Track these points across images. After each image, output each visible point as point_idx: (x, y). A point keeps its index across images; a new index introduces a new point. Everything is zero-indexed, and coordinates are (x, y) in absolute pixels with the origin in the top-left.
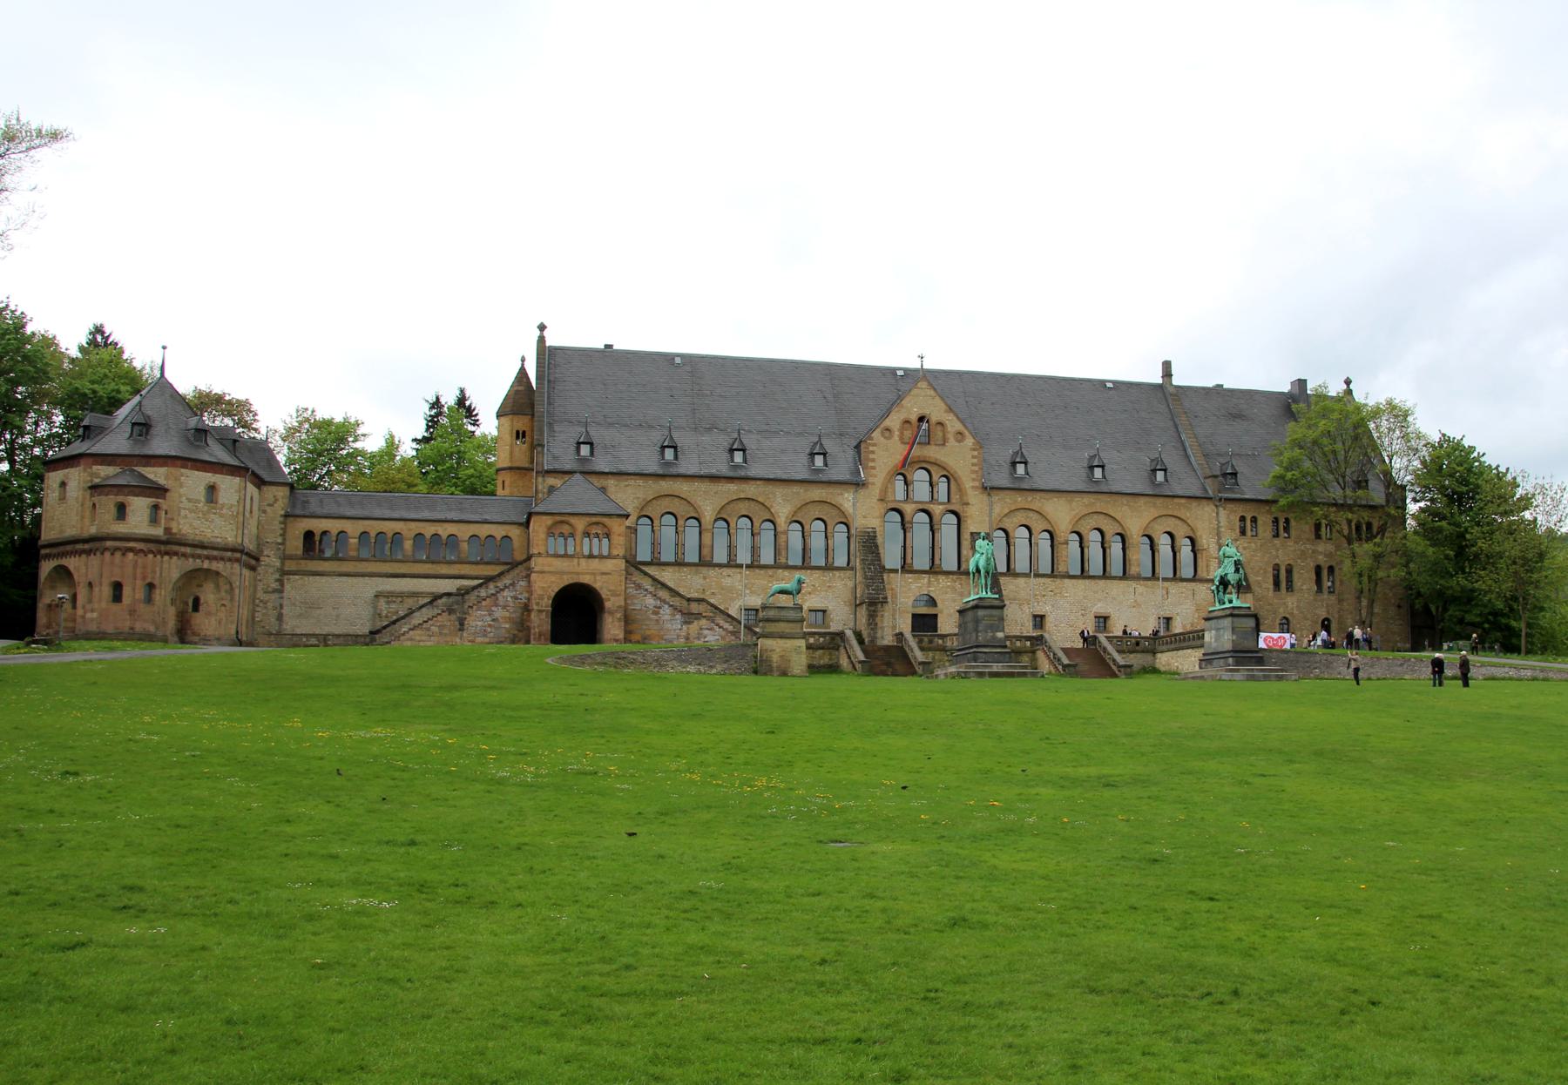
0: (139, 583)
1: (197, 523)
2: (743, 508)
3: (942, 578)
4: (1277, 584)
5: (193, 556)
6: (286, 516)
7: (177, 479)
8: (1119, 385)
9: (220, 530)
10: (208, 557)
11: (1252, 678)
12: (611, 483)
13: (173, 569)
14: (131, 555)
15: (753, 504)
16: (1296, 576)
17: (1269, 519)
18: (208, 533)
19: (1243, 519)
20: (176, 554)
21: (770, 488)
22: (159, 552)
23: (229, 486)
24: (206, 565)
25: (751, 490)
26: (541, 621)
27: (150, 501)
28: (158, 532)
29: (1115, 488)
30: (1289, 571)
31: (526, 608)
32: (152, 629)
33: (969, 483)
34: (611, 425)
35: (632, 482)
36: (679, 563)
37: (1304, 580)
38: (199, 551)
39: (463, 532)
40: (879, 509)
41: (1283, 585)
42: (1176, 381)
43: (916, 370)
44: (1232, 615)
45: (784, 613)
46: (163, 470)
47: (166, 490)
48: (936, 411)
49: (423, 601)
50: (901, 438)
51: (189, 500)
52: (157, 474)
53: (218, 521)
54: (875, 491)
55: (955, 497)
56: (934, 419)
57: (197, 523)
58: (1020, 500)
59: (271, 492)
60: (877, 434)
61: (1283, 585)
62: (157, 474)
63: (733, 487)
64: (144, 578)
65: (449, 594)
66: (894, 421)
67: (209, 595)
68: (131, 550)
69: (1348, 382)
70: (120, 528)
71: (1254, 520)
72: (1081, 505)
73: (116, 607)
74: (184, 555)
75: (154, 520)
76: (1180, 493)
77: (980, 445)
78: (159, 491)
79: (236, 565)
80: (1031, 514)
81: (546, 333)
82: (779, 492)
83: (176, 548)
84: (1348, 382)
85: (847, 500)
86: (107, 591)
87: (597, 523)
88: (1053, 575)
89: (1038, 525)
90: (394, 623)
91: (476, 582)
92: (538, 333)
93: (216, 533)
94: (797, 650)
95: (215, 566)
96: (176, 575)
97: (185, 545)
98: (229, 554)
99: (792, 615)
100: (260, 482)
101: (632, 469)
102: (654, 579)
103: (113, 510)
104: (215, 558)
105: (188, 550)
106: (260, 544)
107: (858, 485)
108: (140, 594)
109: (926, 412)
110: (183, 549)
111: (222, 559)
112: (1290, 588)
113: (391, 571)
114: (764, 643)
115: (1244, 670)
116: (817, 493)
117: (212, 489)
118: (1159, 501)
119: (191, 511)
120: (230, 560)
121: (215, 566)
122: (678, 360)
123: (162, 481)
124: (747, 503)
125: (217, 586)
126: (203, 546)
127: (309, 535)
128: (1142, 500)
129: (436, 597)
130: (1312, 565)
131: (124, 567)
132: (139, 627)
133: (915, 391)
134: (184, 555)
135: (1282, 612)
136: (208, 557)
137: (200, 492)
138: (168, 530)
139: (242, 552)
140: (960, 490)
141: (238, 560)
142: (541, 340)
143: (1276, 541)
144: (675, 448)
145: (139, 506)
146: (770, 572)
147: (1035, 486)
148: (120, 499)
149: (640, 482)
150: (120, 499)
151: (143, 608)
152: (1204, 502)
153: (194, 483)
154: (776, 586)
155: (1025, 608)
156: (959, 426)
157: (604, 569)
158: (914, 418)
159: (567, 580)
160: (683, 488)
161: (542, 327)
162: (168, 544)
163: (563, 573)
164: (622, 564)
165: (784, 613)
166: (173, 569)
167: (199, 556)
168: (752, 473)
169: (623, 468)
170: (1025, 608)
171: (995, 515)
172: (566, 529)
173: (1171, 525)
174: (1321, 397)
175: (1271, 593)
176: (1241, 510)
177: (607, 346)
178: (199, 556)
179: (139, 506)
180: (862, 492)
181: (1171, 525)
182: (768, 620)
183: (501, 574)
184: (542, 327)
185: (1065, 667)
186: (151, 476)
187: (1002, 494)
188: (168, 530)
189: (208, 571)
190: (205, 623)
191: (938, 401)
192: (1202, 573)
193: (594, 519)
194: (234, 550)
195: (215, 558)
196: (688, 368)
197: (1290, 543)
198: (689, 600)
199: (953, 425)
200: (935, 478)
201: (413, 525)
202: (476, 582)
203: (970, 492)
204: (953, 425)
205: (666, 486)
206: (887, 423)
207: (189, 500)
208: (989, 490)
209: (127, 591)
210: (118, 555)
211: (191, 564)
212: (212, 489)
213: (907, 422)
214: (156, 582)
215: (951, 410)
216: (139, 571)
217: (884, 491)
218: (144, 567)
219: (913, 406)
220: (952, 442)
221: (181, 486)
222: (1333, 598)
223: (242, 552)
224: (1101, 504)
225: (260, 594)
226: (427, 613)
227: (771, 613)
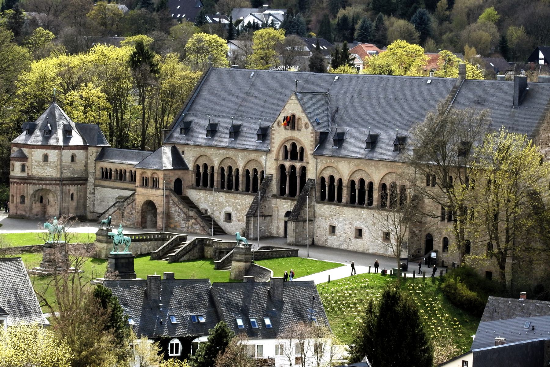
0: (18, 195)
10: (44, 184)
18: (45, 174)
20: (30, 183)
24: (44, 187)
28: (25, 175)
38: (40, 182)
51: (36, 161)
53: (49, 169)
64: (20, 193)
74: (34, 184)
79: (58, 186)
83: (31, 181)
93: (48, 174)
95: (48, 187)
96: (31, 192)
97: (34, 180)
98: (54, 182)
105: (36, 182)
108: (19, 200)
110: (34, 181)
111: (51, 184)
117: (46, 157)
119: (37, 166)
120: (54, 184)
121: (48, 187)
126: (41, 179)
134: (34, 184)
136: (44, 184)
139: (60, 181)
141: (58, 184)
166: (30, 189)
167: (41, 184)
178: (41, 184)
194: (56, 180)
195: (46, 184)
207: (36, 161)
214: (25, 195)
218: (20, 189)
220: (303, 129)
221: (32, 156)
225: (88, 195)
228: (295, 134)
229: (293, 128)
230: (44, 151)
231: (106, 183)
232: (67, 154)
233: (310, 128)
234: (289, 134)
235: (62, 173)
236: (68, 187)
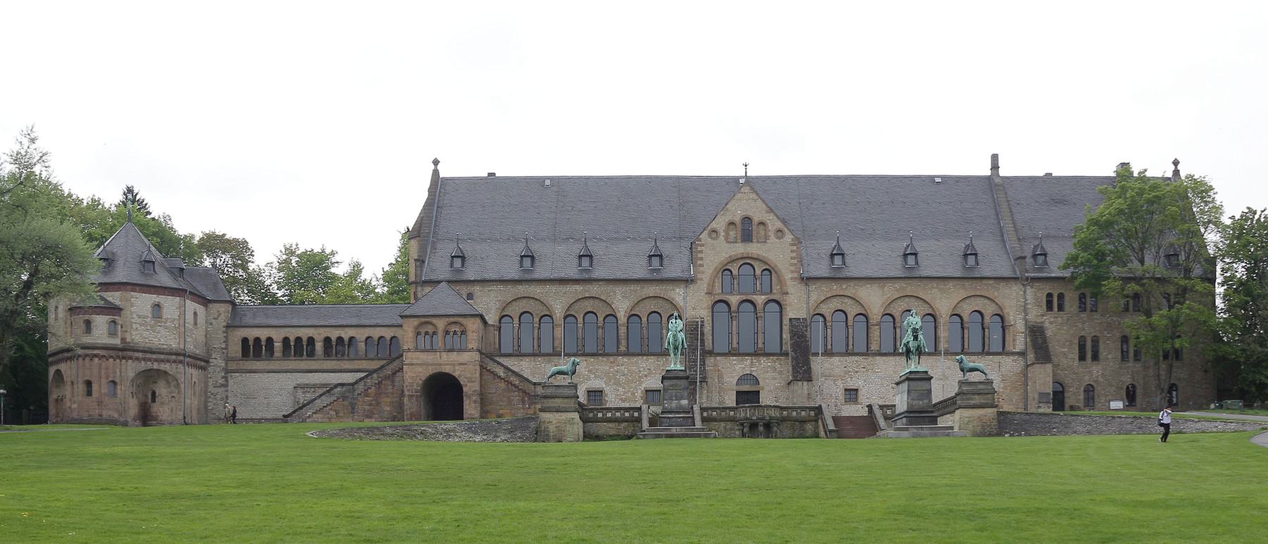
0: (104, 381)
1: (146, 334)
2: (589, 305)
3: (763, 359)
4: (1082, 357)
5: (144, 359)
6: (227, 327)
7: (128, 300)
8: (946, 179)
9: (165, 338)
10: (156, 360)
11: (915, 436)
12: (477, 289)
13: (130, 369)
14: (96, 360)
15: (597, 302)
16: (1102, 347)
17: (1076, 295)
18: (156, 341)
19: (1050, 295)
20: (131, 358)
21: (610, 287)
22: (118, 357)
23: (170, 305)
24: (156, 366)
25: (594, 290)
26: (410, 405)
27: (107, 318)
28: (116, 341)
29: (925, 273)
30: (1096, 341)
31: (402, 394)
32: (116, 416)
33: (788, 276)
34: (484, 240)
35: (494, 288)
36: (519, 354)
37: (1109, 351)
38: (149, 356)
39: (360, 335)
40: (708, 302)
41: (1089, 355)
42: (1003, 172)
43: (736, 179)
44: (908, 379)
45: (560, 391)
46: (118, 294)
47: (121, 309)
48: (758, 212)
49: (321, 391)
50: (726, 239)
51: (139, 317)
52: (114, 297)
53: (163, 332)
54: (703, 286)
55: (776, 288)
56: (756, 220)
57: (146, 334)
58: (835, 288)
59: (215, 308)
60: (704, 236)
61: (1089, 355)
62: (114, 297)
63: (579, 288)
64: (107, 377)
65: (342, 385)
66: (720, 224)
67: (162, 390)
68: (96, 356)
69: (1176, 163)
70: (87, 340)
71: (1061, 296)
72: (891, 291)
73: (89, 400)
75: (112, 334)
76: (988, 274)
77: (797, 241)
78: (114, 310)
80: (846, 300)
81: (439, 167)
82: (619, 290)
83: (130, 353)
84: (1176, 163)
85: (677, 294)
86: (81, 388)
87: (455, 323)
88: (867, 353)
89: (852, 310)
90: (301, 408)
91: (363, 375)
92: (433, 167)
94: (571, 421)
96: (131, 374)
97: (138, 351)
99: (567, 392)
100: (205, 302)
101: (493, 276)
102: (506, 368)
103: (83, 326)
104: (162, 361)
105: (140, 355)
106: (209, 350)
107: (688, 281)
109: (750, 214)
110: (136, 354)
111: (168, 361)
112: (1095, 357)
113: (356, 367)
114: (546, 416)
115: (914, 429)
116: (652, 290)
117: (157, 306)
118: (967, 283)
119: (141, 325)
122: (548, 182)
123: (118, 303)
124: (592, 301)
125: (168, 382)
126: (152, 352)
127: (245, 341)
128: (951, 284)
129: (330, 389)
130: (1118, 335)
131: (93, 369)
132: (105, 414)
133: (739, 196)
134: (137, 359)
135: (1087, 380)
136: (156, 360)
138: (123, 340)
140: (781, 282)
142: (436, 172)
143: (1083, 315)
144: (591, 257)
145: (101, 322)
146: (611, 359)
147: (849, 275)
148: (87, 317)
149: (501, 287)
150: (87, 317)
152: (1012, 283)
153: (141, 303)
154: (554, 369)
155: (840, 383)
156: (779, 225)
157: (462, 361)
158: (737, 219)
159: (431, 370)
160: (536, 290)
161: (436, 162)
162: (125, 351)
163: (428, 365)
164: (476, 356)
165: (560, 391)
166: (130, 369)
167: (150, 360)
168: (595, 275)
169: (487, 276)
170: (840, 383)
171: (812, 302)
172: (430, 329)
173: (979, 304)
174: (1142, 178)
175: (1076, 362)
176: (1047, 288)
177: (490, 174)
178: (150, 360)
179: (101, 322)
180: (692, 287)
181: (979, 304)
182: (545, 397)
183: (383, 367)
184: (436, 162)
185: (831, 431)
186: (110, 299)
187: (818, 283)
188: (123, 340)
189: (158, 370)
190: (161, 410)
191: (759, 202)
192: (1009, 348)
193: (452, 320)
195: (162, 361)
196: (555, 189)
197: (1096, 316)
198: (535, 384)
199: (774, 223)
200: (758, 272)
201: (322, 330)
202: (363, 375)
203: (789, 283)
204: (774, 223)
205: (522, 290)
206: (714, 225)
207: (139, 317)
208: (807, 280)
209: (95, 387)
210: (87, 360)
211: (143, 366)
212: (157, 306)
213: (732, 223)
214: (117, 380)
215: (771, 210)
216: (103, 372)
217: (712, 284)
218: (107, 368)
219: (736, 211)
220: (773, 238)
221: (132, 305)
222: (1138, 365)
223: (184, 355)
224: (911, 288)
226: (326, 400)
227: (549, 391)
228: (753, 249)
229: (747, 237)
233: (789, 237)
234: (741, 249)
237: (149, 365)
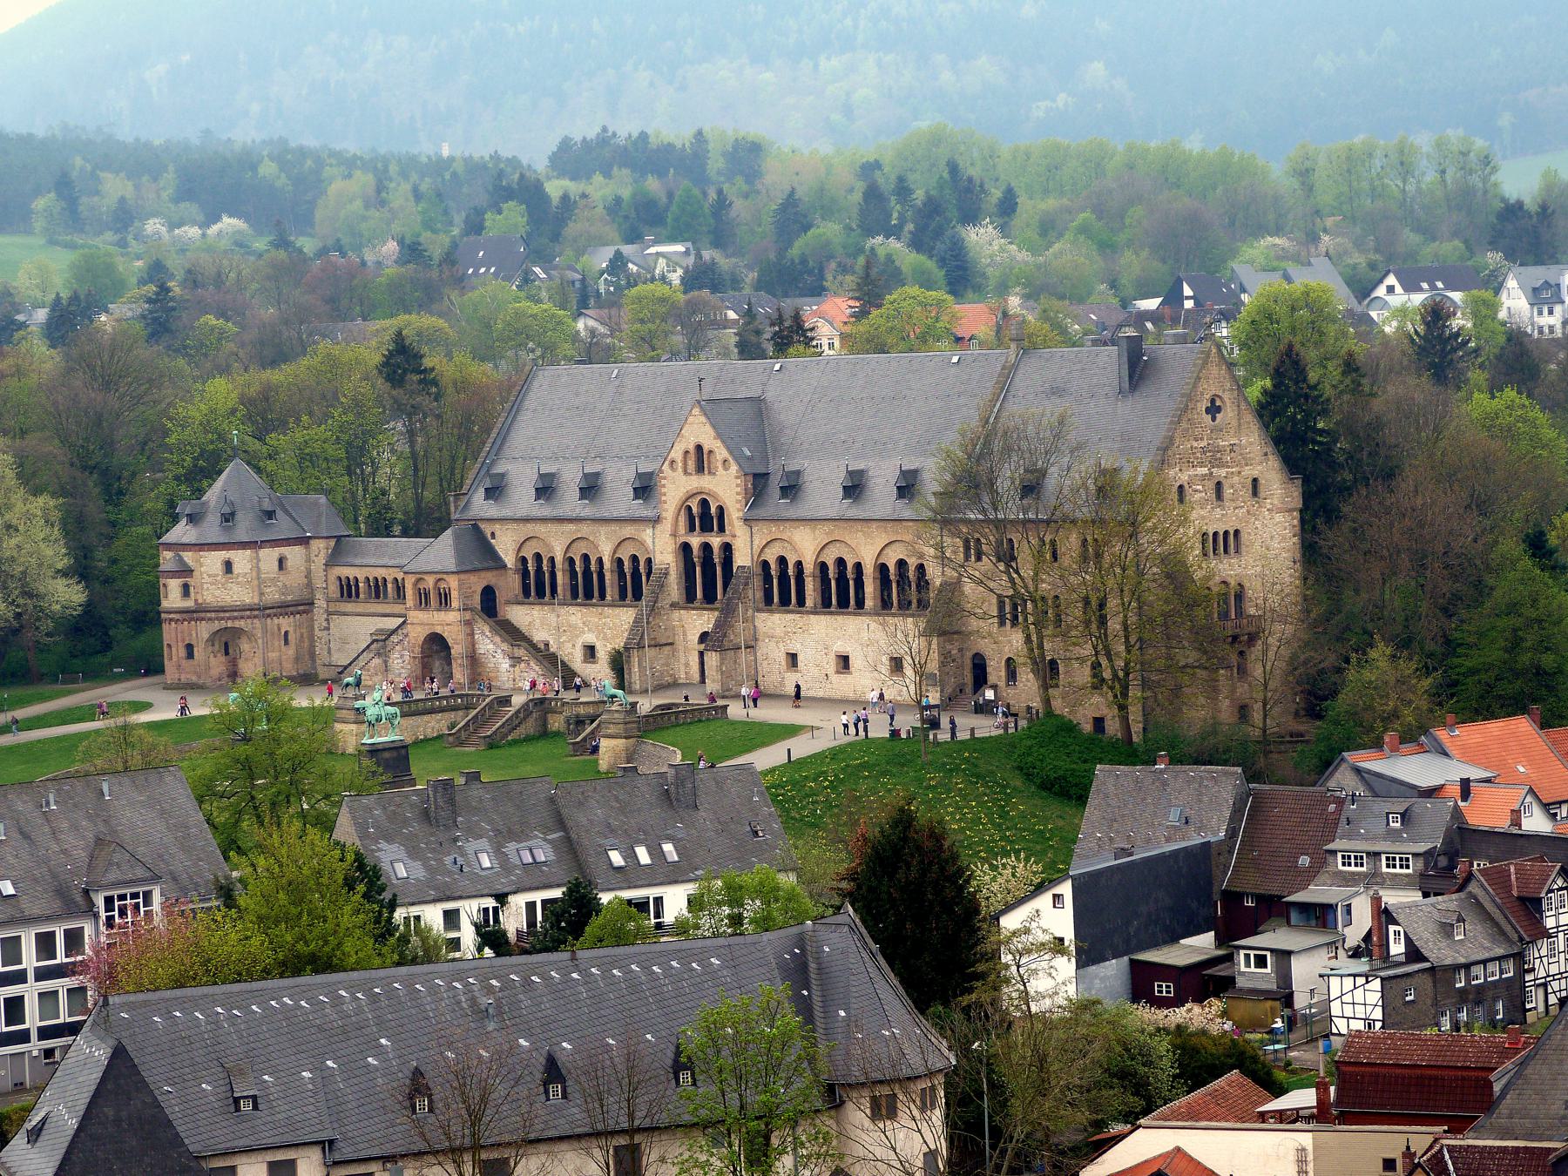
7: (197, 561)
9: (238, 593)
24: (230, 624)
28: (189, 603)
32: (194, 679)
57: (217, 593)
96: (206, 636)
108: (183, 652)
117: (228, 566)
121: (237, 624)
137: (218, 568)
151: (184, 663)
166: (204, 630)
204: (721, 453)
211: (217, 625)
220: (721, 470)
225: (317, 632)
229: (700, 469)
230: (224, 555)
231: (349, 607)
232: (269, 556)
233: (734, 468)
235: (262, 594)
236: (276, 621)
237: (223, 624)
